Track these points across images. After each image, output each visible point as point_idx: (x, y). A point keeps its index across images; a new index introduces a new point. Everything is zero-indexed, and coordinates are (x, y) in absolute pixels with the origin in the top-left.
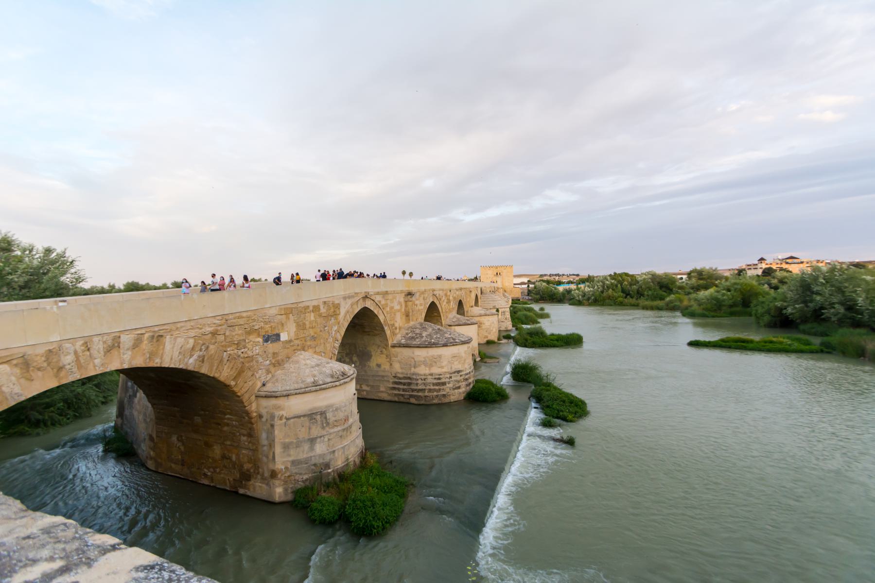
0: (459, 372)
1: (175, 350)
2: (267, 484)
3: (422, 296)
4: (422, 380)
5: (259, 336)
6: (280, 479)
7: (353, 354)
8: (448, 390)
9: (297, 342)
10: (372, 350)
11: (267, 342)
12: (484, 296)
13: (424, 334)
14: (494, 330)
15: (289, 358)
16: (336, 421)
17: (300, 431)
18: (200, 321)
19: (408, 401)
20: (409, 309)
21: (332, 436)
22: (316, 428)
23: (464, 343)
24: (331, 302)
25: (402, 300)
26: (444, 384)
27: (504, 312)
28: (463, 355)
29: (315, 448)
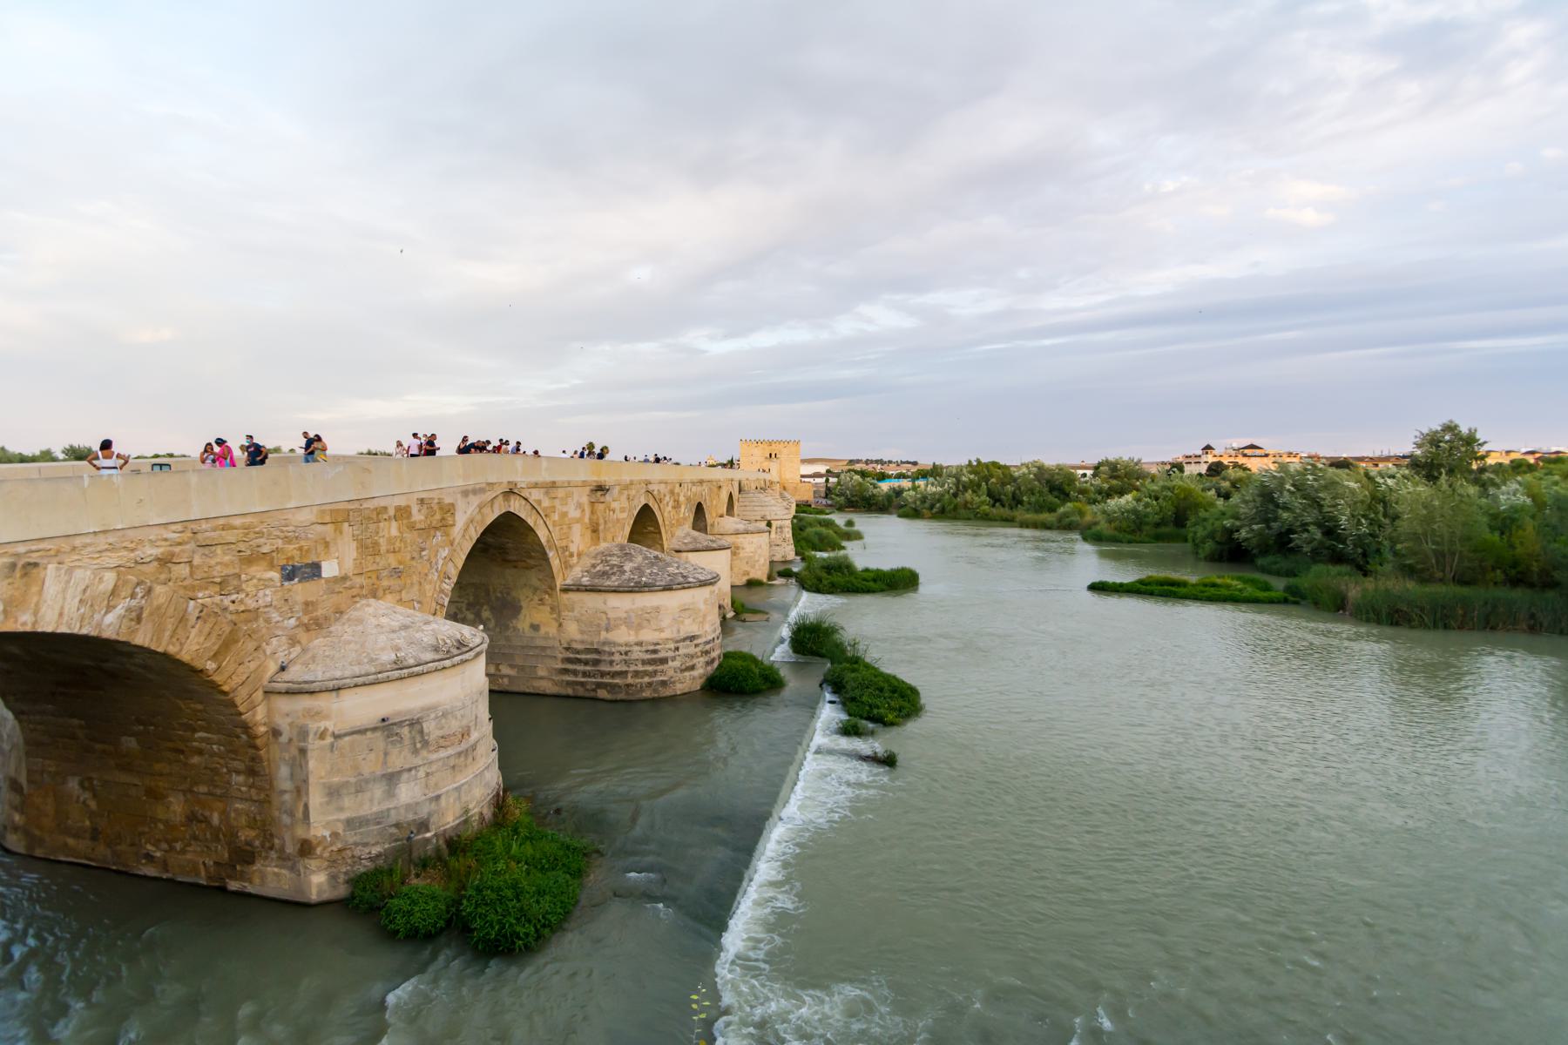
0: (692, 638)
1: (69, 596)
2: (292, 869)
3: (626, 492)
4: (621, 654)
5: (272, 566)
6: (321, 857)
7: (482, 606)
8: (671, 673)
9: (359, 580)
10: (522, 598)
11: (292, 579)
12: (744, 496)
13: (628, 567)
14: (762, 561)
15: (342, 613)
16: (442, 737)
17: (364, 759)
18: (131, 533)
19: (592, 694)
20: (598, 519)
21: (434, 768)
22: (400, 752)
23: (705, 585)
24: (436, 501)
25: (585, 500)
26: (664, 661)
27: (781, 527)
28: (702, 606)
29: (397, 791)
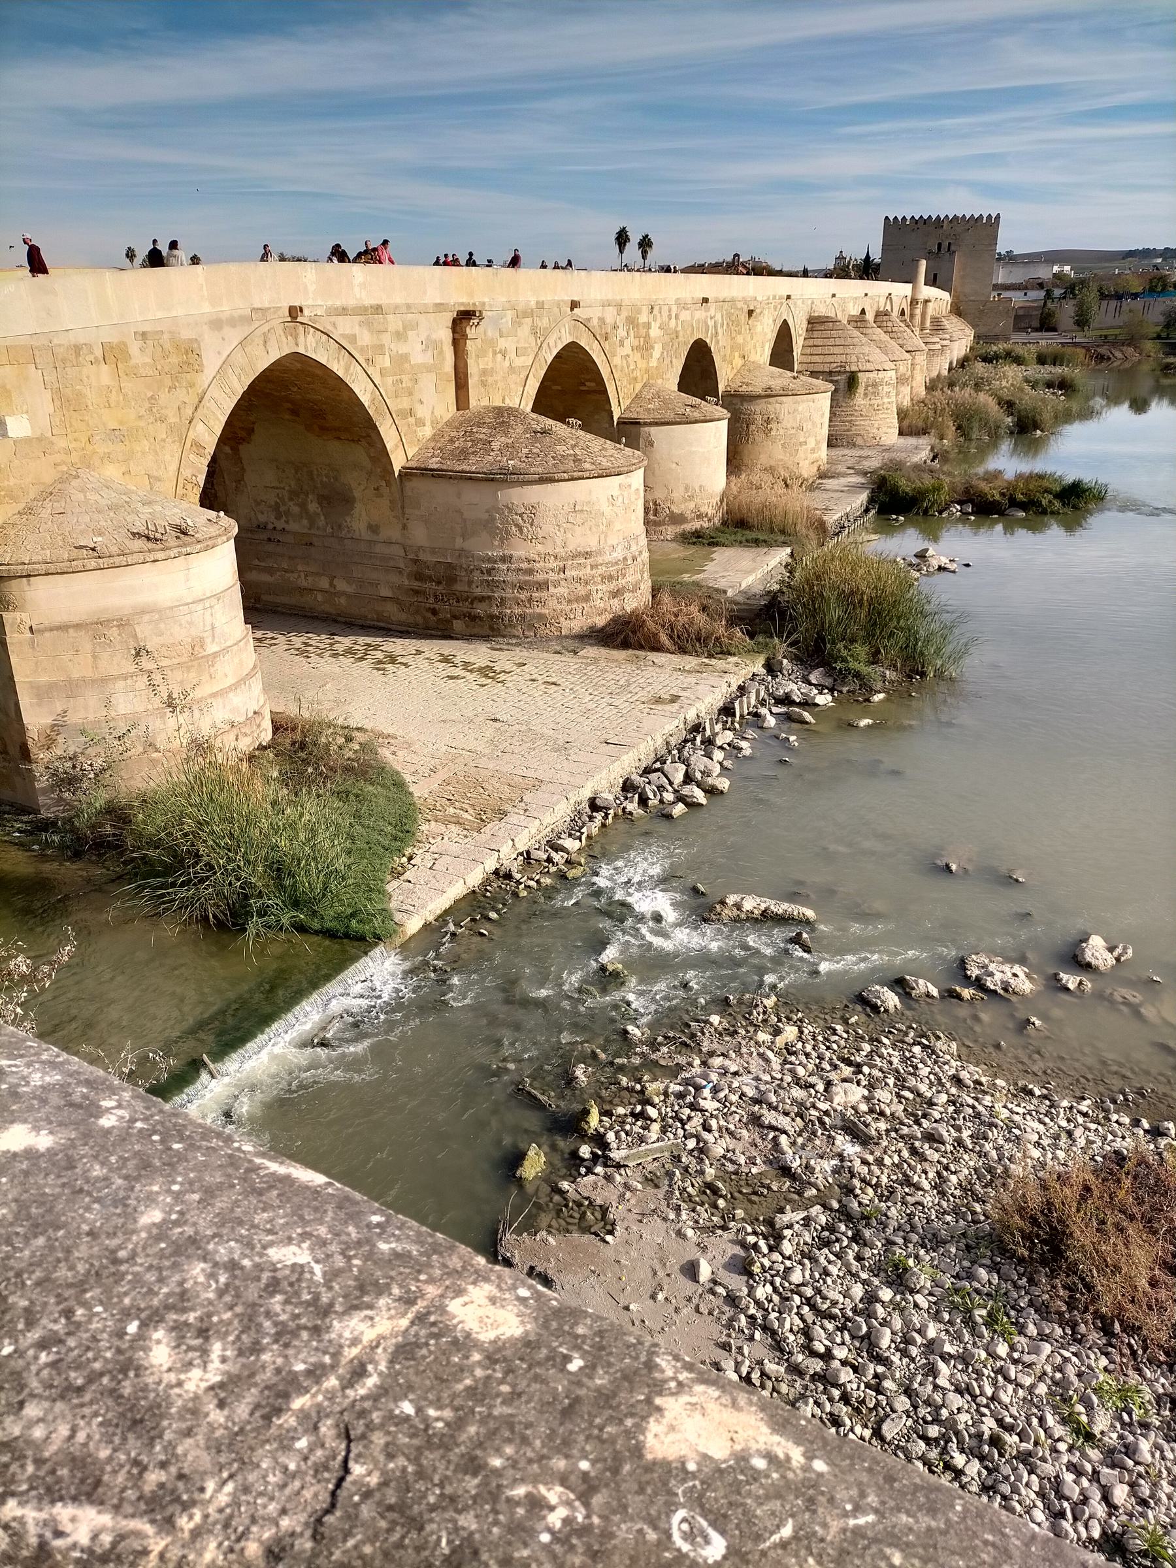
0: (587, 555)
8: (553, 604)
26: (543, 586)
